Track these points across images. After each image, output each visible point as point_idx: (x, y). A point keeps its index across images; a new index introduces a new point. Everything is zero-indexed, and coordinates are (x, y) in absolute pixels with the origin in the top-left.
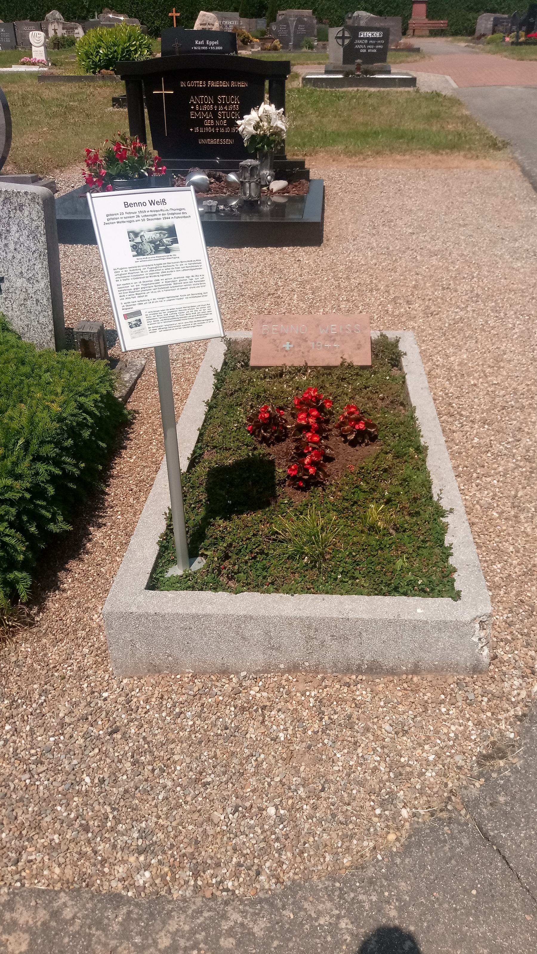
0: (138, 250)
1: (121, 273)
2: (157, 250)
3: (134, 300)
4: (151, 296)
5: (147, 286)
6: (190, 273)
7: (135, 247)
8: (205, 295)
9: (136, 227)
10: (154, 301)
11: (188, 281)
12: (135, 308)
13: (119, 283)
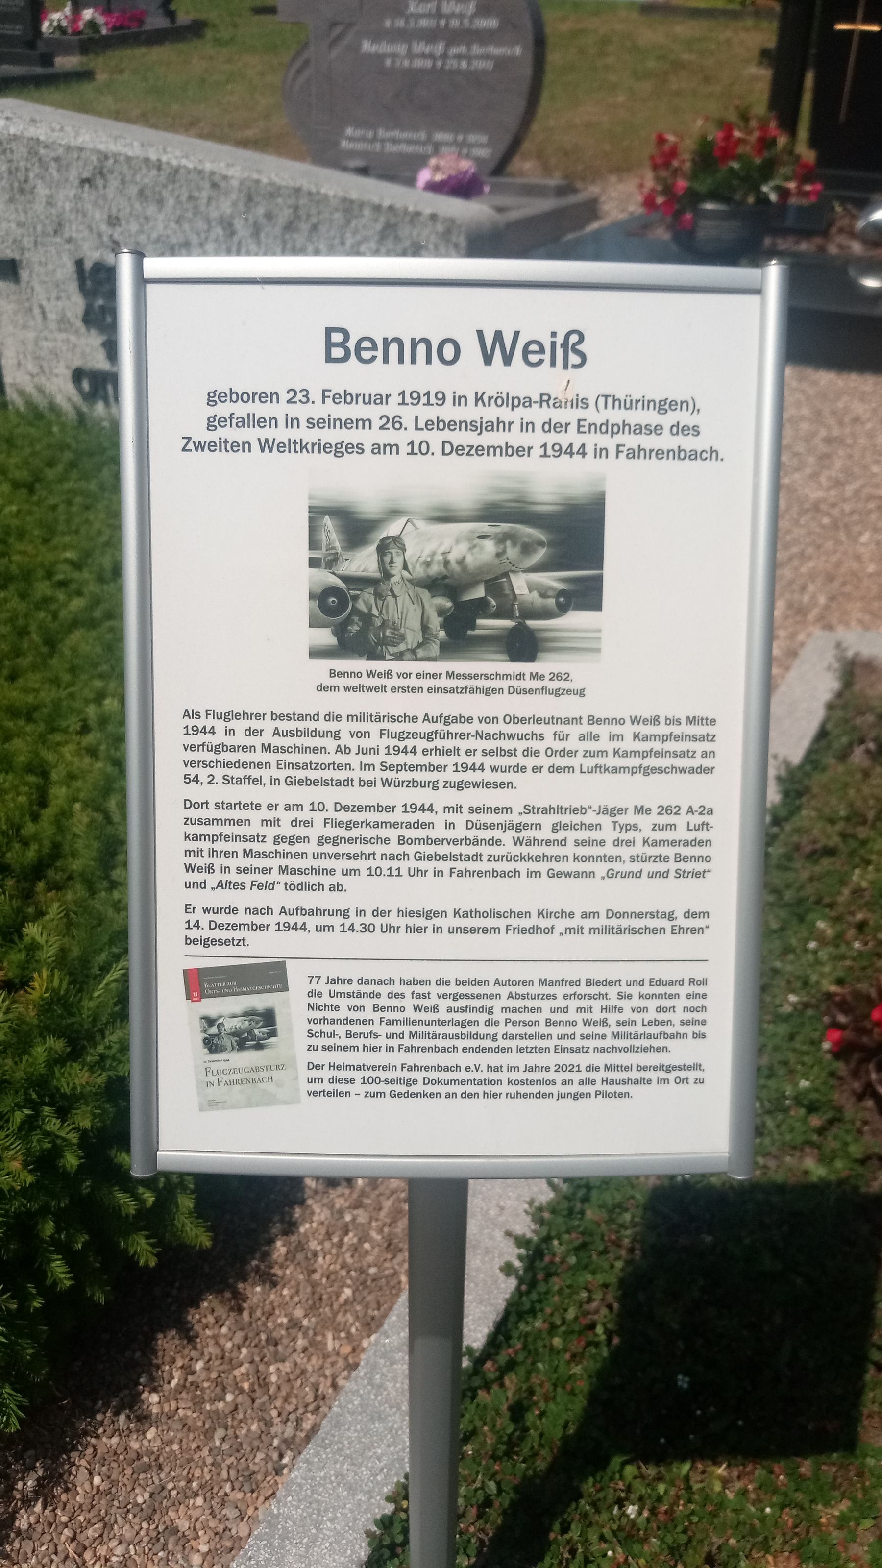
0: (350, 622)
1: (218, 741)
2: (459, 633)
3: (259, 898)
4: (362, 892)
5: (352, 838)
6: (626, 790)
7: (331, 605)
8: (693, 923)
9: (362, 483)
10: (378, 921)
11: (608, 833)
12: (261, 947)
13: (196, 793)
